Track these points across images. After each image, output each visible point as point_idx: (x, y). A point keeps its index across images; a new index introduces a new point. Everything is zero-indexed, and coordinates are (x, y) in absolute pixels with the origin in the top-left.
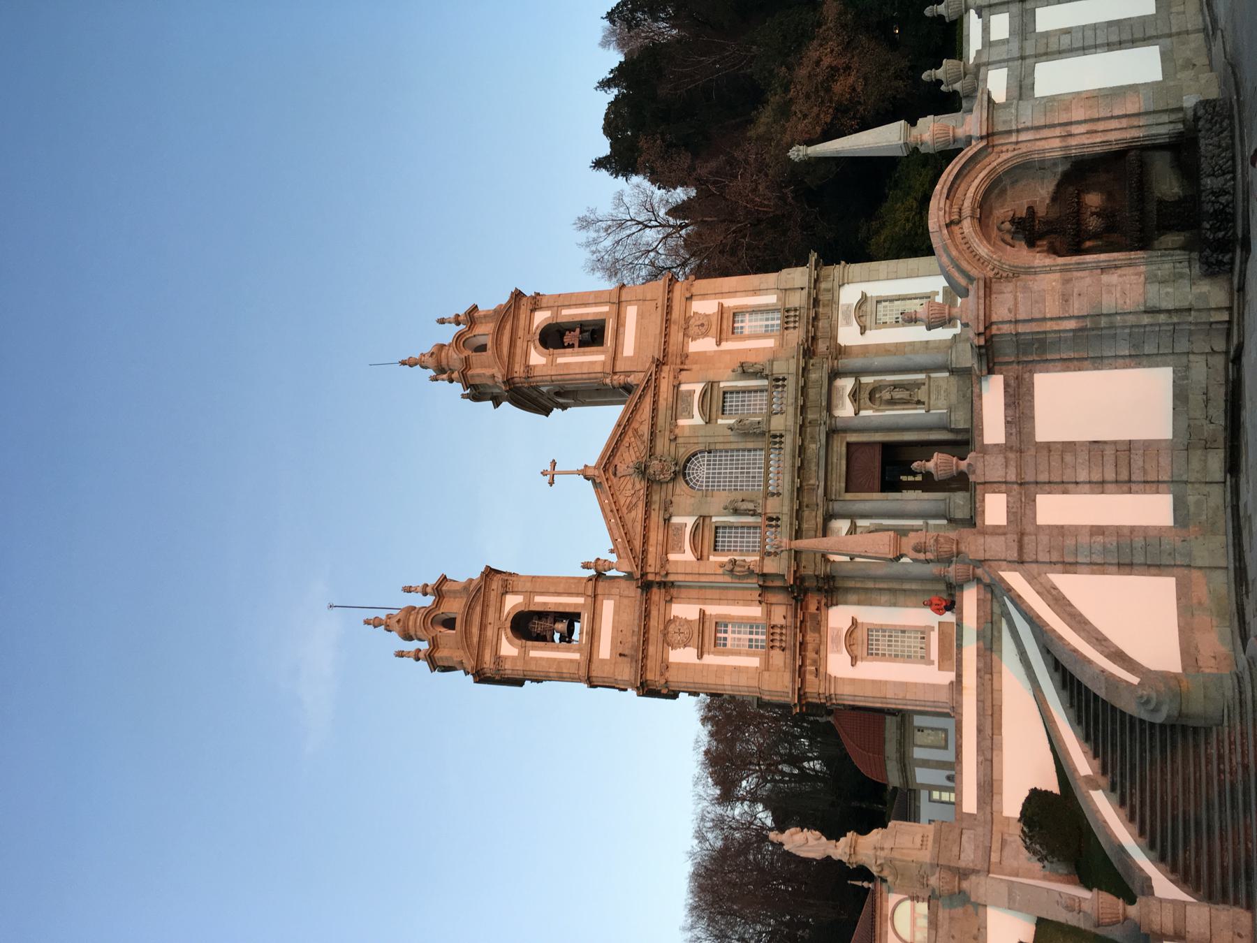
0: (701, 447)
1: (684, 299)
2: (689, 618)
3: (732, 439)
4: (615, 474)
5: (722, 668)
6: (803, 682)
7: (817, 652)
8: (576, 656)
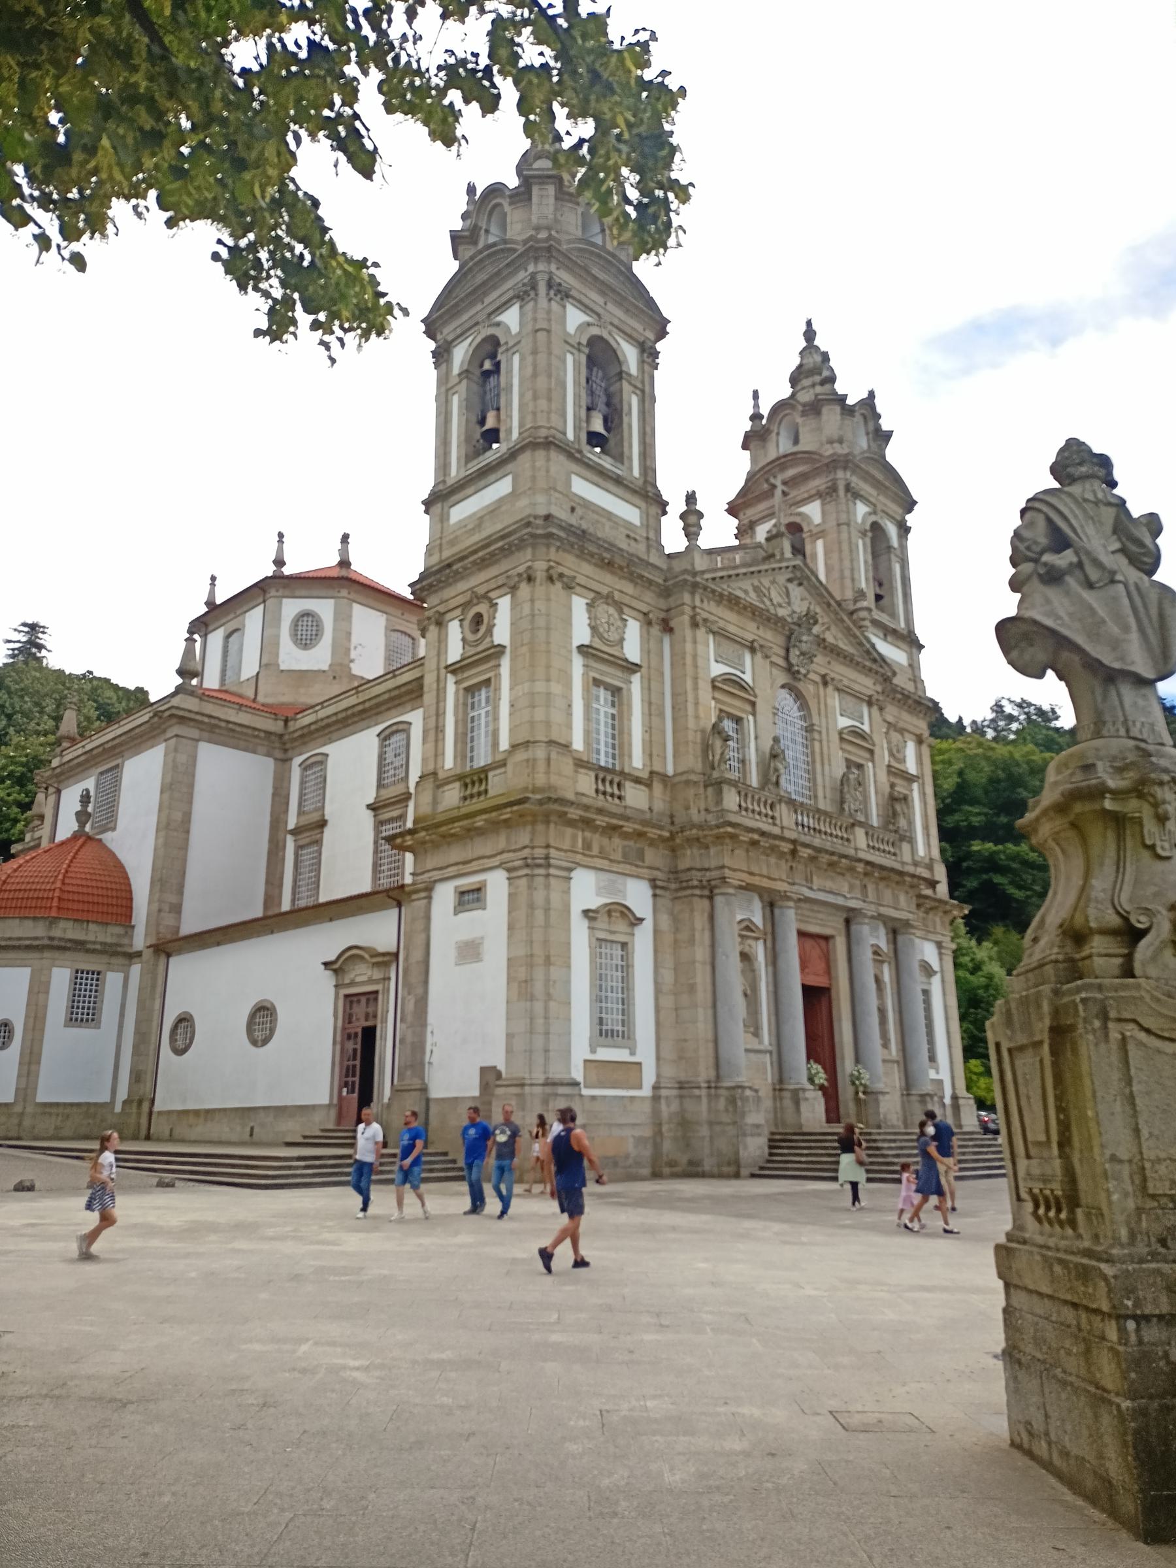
0: (815, 720)
1: (918, 732)
2: (625, 644)
3: (827, 767)
4: (790, 580)
5: (568, 685)
6: (571, 823)
7: (603, 855)
8: (570, 435)
